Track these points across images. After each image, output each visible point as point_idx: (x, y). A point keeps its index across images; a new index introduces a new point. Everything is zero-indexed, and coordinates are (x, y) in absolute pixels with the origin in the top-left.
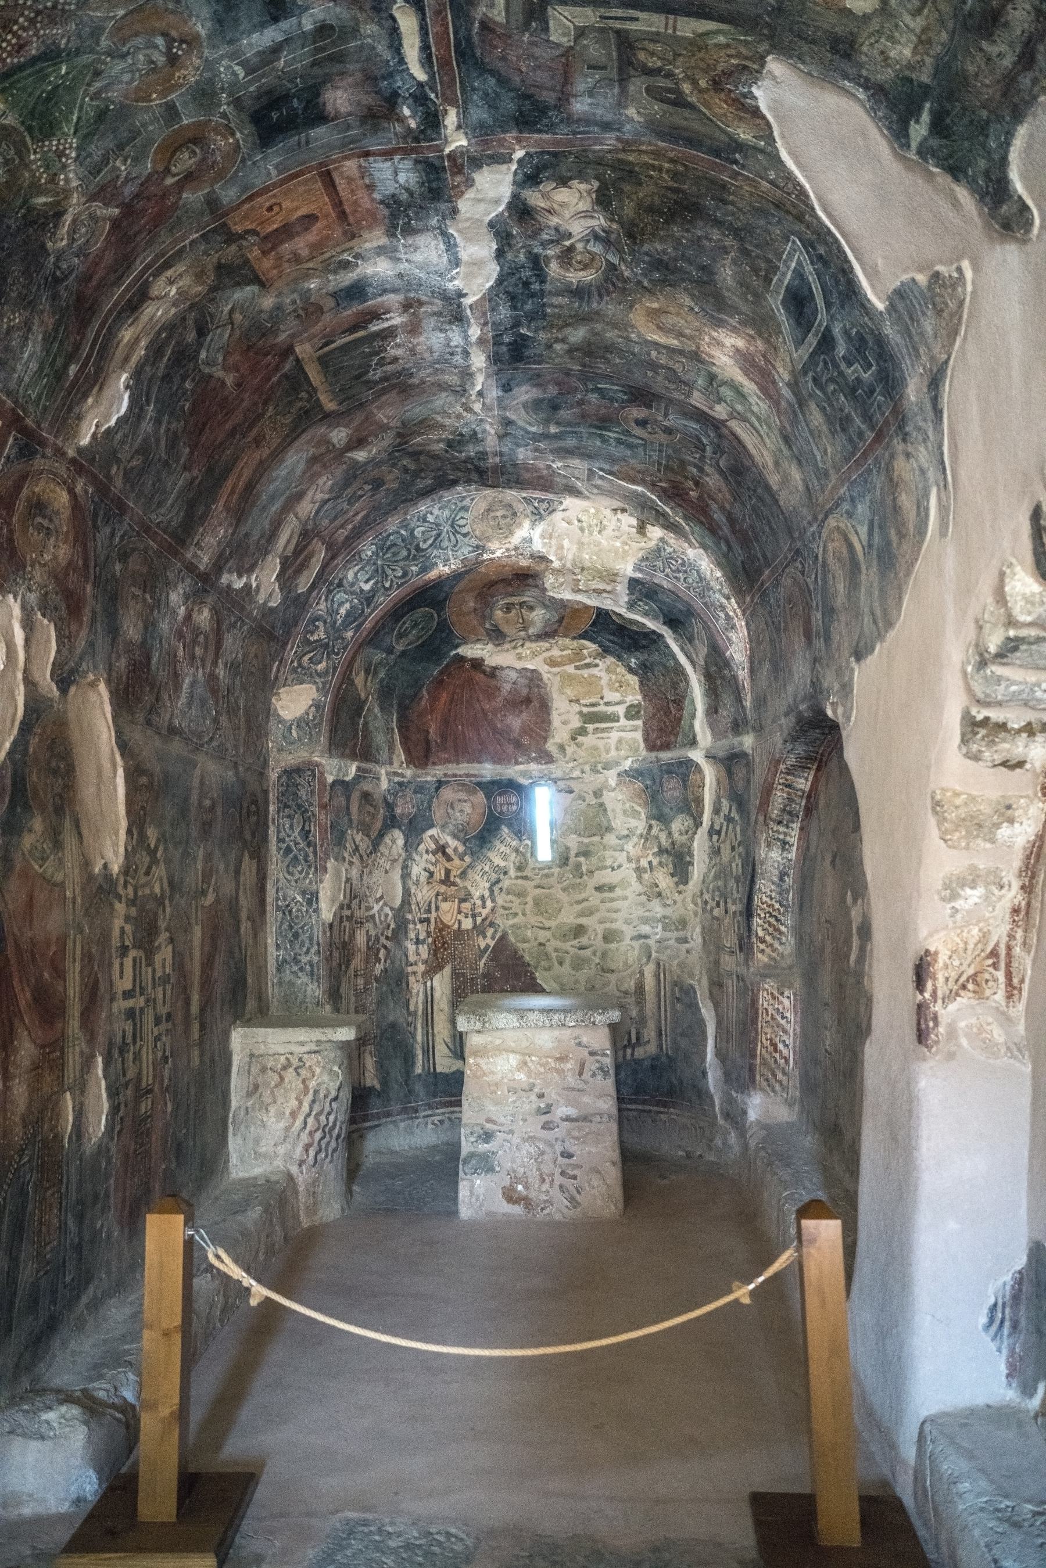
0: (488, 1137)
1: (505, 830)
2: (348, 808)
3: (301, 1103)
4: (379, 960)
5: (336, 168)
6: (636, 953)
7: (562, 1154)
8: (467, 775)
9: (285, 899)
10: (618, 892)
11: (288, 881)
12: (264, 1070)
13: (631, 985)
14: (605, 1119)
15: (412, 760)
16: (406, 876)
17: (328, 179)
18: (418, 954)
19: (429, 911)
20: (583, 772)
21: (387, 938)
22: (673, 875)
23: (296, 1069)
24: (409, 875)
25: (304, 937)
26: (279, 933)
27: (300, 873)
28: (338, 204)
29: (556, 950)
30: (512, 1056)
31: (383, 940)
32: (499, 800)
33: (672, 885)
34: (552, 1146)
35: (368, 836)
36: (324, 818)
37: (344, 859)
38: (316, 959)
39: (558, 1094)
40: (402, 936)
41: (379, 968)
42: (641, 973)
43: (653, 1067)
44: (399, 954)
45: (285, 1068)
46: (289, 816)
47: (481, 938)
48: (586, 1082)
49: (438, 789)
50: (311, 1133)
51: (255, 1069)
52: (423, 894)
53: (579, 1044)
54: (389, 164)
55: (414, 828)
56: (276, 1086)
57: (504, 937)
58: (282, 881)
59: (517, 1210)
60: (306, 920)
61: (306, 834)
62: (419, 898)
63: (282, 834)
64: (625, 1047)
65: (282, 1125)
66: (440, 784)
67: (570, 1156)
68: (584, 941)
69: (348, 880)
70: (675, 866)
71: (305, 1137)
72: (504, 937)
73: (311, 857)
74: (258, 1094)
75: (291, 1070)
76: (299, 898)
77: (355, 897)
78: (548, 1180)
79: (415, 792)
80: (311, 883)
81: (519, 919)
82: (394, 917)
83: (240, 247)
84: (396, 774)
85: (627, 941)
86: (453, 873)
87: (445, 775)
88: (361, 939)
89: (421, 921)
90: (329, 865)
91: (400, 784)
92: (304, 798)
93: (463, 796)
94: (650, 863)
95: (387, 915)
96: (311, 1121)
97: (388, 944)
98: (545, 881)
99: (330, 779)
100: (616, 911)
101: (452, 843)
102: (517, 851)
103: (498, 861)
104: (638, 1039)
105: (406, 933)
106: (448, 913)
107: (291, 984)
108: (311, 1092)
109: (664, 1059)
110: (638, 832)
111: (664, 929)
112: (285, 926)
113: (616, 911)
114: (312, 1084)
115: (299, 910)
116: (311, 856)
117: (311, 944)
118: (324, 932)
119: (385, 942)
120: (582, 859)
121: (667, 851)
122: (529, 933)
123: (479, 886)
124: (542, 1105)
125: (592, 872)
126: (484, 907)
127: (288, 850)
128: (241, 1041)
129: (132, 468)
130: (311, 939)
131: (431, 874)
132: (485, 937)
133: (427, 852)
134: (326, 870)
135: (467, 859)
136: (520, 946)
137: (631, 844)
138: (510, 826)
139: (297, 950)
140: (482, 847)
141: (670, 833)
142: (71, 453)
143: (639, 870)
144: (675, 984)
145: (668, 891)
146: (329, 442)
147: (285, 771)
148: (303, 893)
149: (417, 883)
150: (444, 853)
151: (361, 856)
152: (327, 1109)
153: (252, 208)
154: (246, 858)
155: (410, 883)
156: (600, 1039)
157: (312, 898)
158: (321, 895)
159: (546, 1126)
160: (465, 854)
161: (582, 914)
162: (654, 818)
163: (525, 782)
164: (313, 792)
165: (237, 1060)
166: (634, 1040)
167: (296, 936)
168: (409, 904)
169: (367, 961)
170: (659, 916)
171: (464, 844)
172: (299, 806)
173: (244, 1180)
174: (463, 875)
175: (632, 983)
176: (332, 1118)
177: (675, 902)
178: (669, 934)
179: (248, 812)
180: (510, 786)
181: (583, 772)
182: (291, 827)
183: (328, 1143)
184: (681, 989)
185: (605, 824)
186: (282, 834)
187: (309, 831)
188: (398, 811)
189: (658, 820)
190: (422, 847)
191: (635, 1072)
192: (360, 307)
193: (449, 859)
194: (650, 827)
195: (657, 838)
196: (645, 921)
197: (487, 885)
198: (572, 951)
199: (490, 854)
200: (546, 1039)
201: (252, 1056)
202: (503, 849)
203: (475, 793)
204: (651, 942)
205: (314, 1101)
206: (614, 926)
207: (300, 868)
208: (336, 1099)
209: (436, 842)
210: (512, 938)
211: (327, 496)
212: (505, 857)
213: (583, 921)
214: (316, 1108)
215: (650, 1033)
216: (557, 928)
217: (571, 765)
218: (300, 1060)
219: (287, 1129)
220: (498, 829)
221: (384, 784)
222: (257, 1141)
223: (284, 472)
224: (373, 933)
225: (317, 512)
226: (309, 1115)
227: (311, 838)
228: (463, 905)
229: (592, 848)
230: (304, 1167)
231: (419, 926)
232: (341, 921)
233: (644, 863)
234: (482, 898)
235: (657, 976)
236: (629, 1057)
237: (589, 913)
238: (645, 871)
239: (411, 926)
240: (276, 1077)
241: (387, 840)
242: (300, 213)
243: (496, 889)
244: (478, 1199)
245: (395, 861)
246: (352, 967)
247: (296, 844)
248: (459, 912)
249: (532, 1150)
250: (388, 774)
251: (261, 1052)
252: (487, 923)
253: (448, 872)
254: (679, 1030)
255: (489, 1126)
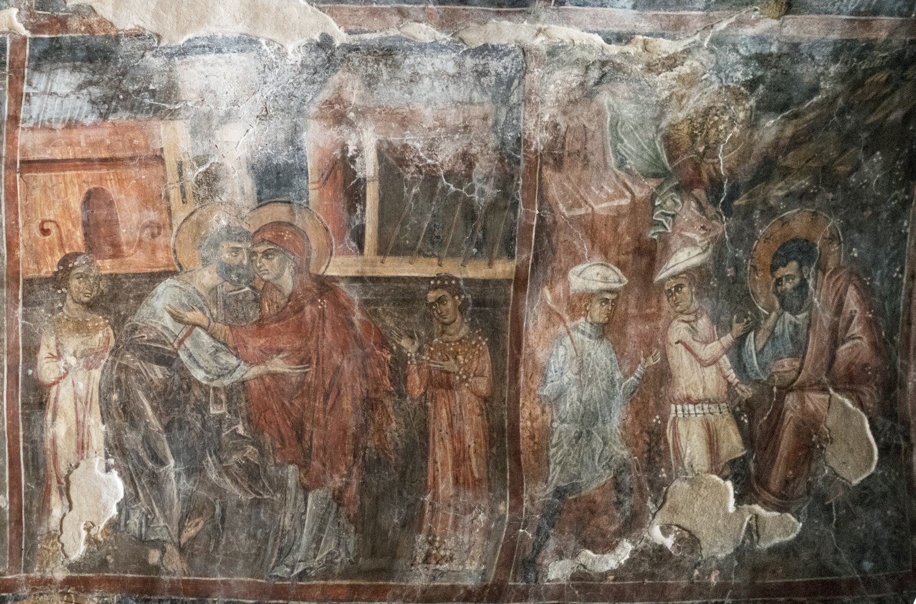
5: (24, 153)
17: (29, 165)
28: (87, 163)
54: (34, 99)
83: (83, 277)
129: (194, 539)
142: (60, 575)
146: (589, 296)
153: (29, 249)
192: (313, 176)
211: (728, 339)
223: (570, 375)
225: (740, 367)
242: (76, 203)
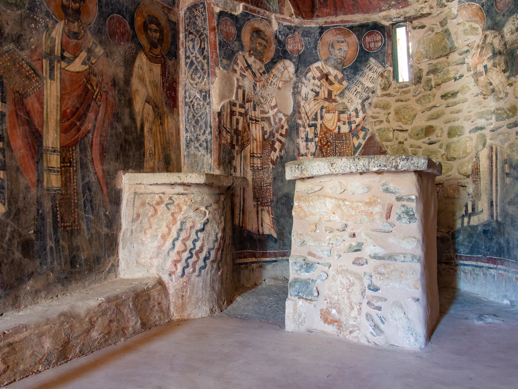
0: (308, 266)
1: (372, 61)
2: (239, 37)
3: (170, 230)
4: (275, 150)
6: (474, 143)
7: (369, 286)
8: (342, 22)
9: (190, 97)
10: (460, 96)
11: (191, 84)
12: (143, 204)
13: (468, 168)
14: (409, 258)
15: (299, 12)
16: (296, 93)
18: (307, 149)
19: (316, 119)
20: (431, 8)
21: (281, 135)
22: (504, 71)
23: (167, 205)
24: (299, 93)
25: (201, 123)
26: (187, 121)
27: (199, 78)
29: (411, 146)
30: (328, 200)
31: (277, 136)
32: (368, 39)
33: (504, 80)
34: (360, 279)
35: (261, 60)
36: (213, 38)
37: (235, 71)
38: (209, 137)
39: (367, 235)
40: (294, 135)
41: (274, 155)
42: (477, 157)
43: (485, 232)
44: (292, 147)
45: (158, 204)
46: (193, 40)
47: (355, 138)
48: (392, 225)
49: (321, 33)
50: (178, 253)
51: (138, 203)
52: (310, 107)
53: (387, 190)
55: (303, 62)
56: (152, 216)
57: (372, 138)
58: (189, 85)
59: (331, 329)
60: (203, 111)
61: (202, 50)
62: (308, 108)
63: (188, 53)
64: (463, 216)
65: (156, 244)
66: (322, 30)
67: (376, 289)
68: (433, 138)
69: (239, 87)
70: (506, 63)
71: (173, 255)
72: (372, 138)
73: (206, 67)
74: (139, 221)
75: (163, 205)
76: (198, 96)
77: (249, 101)
78: (356, 308)
79: (303, 36)
80: (205, 84)
81: (385, 125)
82: (288, 121)
84: (284, 19)
85: (467, 131)
86: (334, 93)
87: (326, 23)
88: (256, 131)
89: (310, 126)
90: (217, 71)
91: (289, 28)
92: (200, 25)
93: (341, 38)
94: (485, 67)
95: (281, 120)
96: (178, 244)
97: (283, 139)
98: (403, 97)
99: (217, 10)
100: (458, 112)
101: (333, 72)
102: (382, 75)
103: (368, 84)
104: (473, 209)
105: (298, 133)
106: (330, 120)
107: (195, 156)
108: (179, 223)
109: (494, 224)
110: (476, 44)
111: (497, 120)
112: (191, 116)
113: (458, 112)
114: (180, 217)
115: (198, 104)
116: (206, 65)
117: (206, 127)
118: (214, 119)
119: (280, 138)
120: (431, 76)
121: (500, 53)
122: (391, 135)
123: (353, 102)
124: (354, 244)
125: (439, 85)
126: (357, 117)
127: (192, 63)
128: (128, 182)
130: (206, 123)
131: (317, 94)
132: (358, 138)
133: (314, 78)
134: (215, 74)
135: (345, 83)
136: (385, 144)
137: (470, 56)
138: (376, 57)
139: (198, 132)
140: (355, 74)
141: (502, 37)
143: (477, 75)
144: (505, 162)
145: (500, 87)
147: (188, 9)
148: (201, 91)
149: (306, 99)
150: (327, 79)
151: (254, 74)
152: (193, 236)
154: (142, 60)
155: (300, 98)
156: (408, 186)
157: (206, 95)
158: (212, 92)
159: (357, 262)
160: (343, 79)
161: (431, 118)
162: (489, 28)
163: (386, 23)
164: (205, 20)
165: (126, 197)
166: (470, 210)
167: (197, 122)
168: (300, 113)
169: (263, 147)
170: (492, 109)
171: (342, 73)
172: (198, 32)
173: (128, 280)
174: (342, 94)
175: (470, 167)
176: (198, 244)
177: (507, 94)
178: (501, 123)
179: (145, 27)
180: (376, 27)
181: (431, 8)
182: (193, 47)
183: (195, 263)
184: (511, 166)
185: (449, 45)
186: (188, 53)
187: (204, 48)
188: (289, 48)
189: (493, 29)
190: (310, 75)
191: (471, 236)
193: (331, 83)
194: (486, 37)
195: (491, 44)
196: (481, 115)
197: (360, 101)
198: (425, 146)
199: (363, 80)
200: (357, 185)
201: (135, 193)
202: (371, 74)
203: (348, 34)
204: (486, 132)
205: (181, 230)
206: (456, 124)
207: (198, 75)
208: (202, 230)
209: (321, 71)
210: (378, 138)
212: (373, 81)
213: (432, 123)
214: (183, 235)
215: (483, 205)
216: (412, 129)
217: (423, 5)
218: (170, 198)
219: (159, 248)
220: (367, 60)
221: (275, 27)
222: (138, 255)
224: (267, 129)
226: (177, 239)
227: (205, 53)
228: (341, 115)
229: (438, 67)
230: (173, 277)
231: (308, 129)
232: (232, 113)
233: (480, 68)
234: (356, 110)
235: (490, 158)
236: (465, 224)
237: (437, 116)
238: (481, 74)
239: (301, 129)
240: (152, 209)
241: (280, 66)
243: (366, 103)
244: (300, 316)
245: (286, 82)
246: (248, 148)
247: (196, 58)
248: (339, 120)
249: (345, 281)
250: (277, 19)
251: (142, 191)
252: (360, 127)
253: (330, 93)
254: (508, 200)
255: (310, 259)
